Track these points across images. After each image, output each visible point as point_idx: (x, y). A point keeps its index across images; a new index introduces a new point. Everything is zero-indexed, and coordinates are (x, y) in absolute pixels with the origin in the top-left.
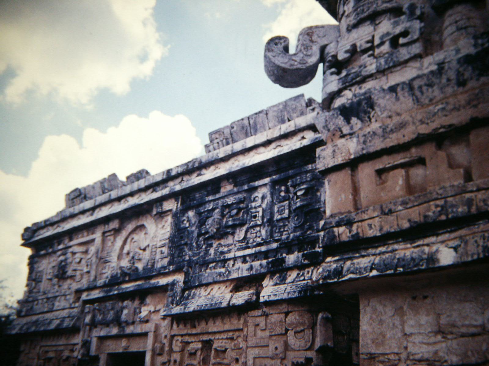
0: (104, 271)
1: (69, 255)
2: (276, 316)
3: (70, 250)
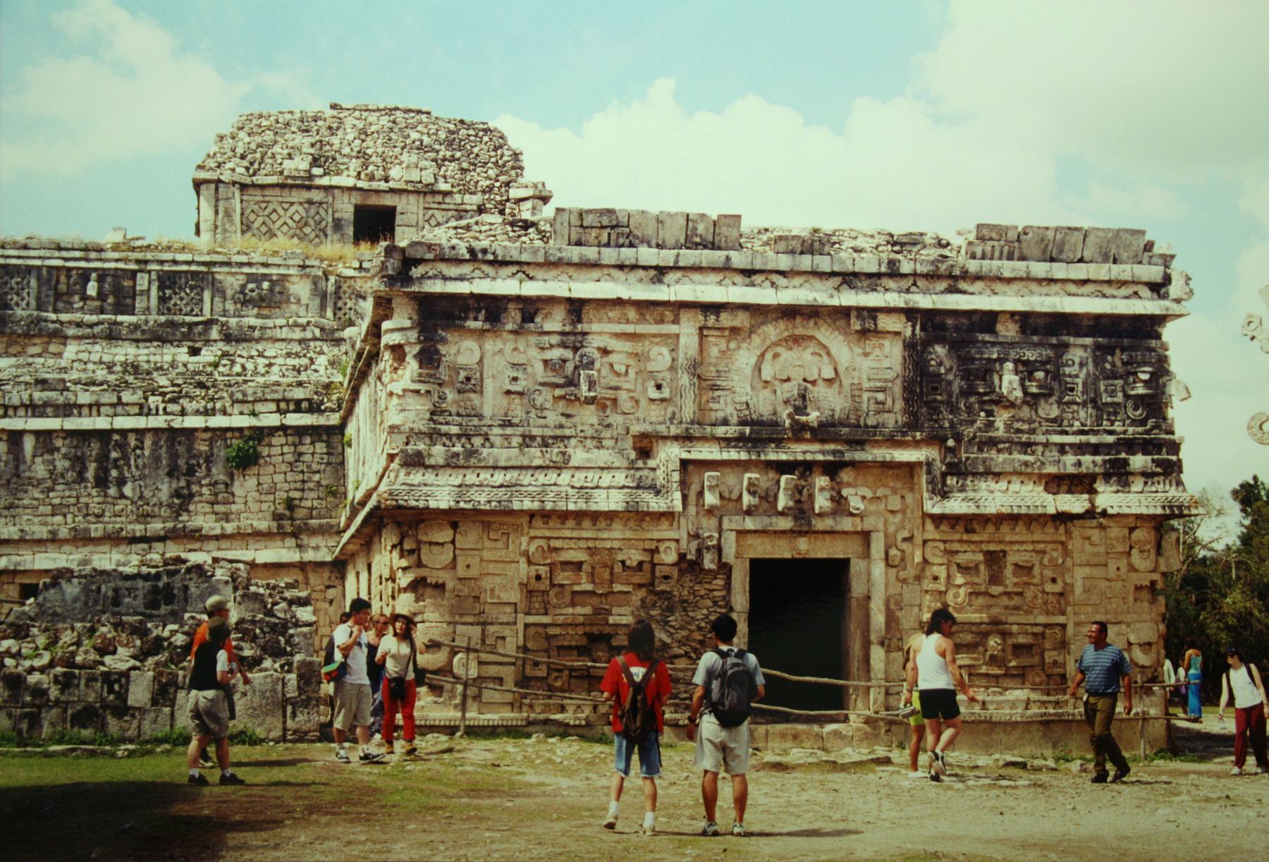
0: (712, 405)
1: (591, 350)
2: (1116, 530)
3: (594, 342)
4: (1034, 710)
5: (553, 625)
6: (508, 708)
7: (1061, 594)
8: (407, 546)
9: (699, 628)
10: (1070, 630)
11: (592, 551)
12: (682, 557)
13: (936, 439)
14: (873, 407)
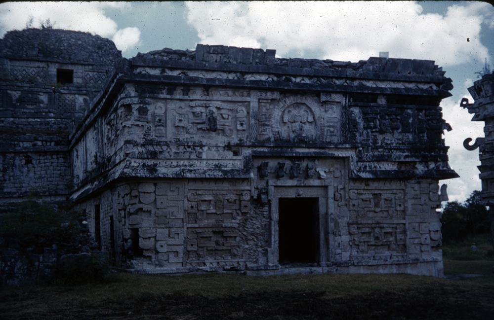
4: (395, 259)
5: (199, 228)
6: (181, 265)
7: (403, 211)
8: (133, 194)
9: (258, 228)
10: (407, 225)
11: (215, 195)
12: (252, 197)
13: (354, 147)
14: (329, 134)
